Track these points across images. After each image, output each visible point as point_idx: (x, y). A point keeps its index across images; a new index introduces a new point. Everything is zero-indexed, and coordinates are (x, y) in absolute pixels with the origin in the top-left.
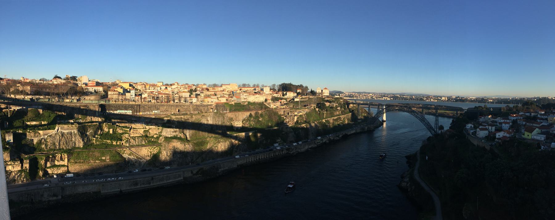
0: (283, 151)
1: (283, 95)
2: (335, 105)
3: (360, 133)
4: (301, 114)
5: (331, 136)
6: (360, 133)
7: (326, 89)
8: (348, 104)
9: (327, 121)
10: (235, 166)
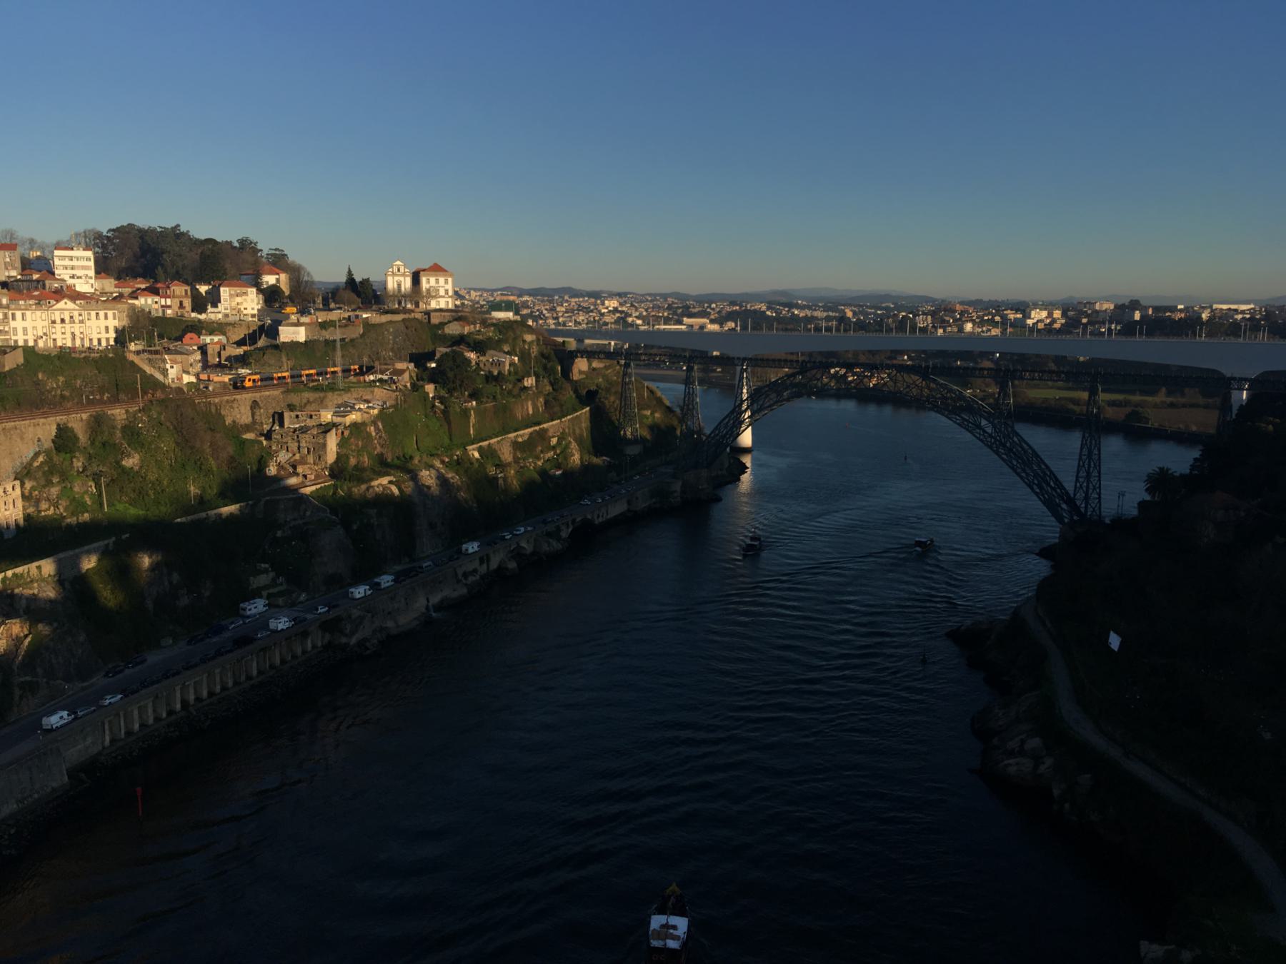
0: (305, 634)
1: (199, 305)
2: (508, 361)
4: (353, 417)
5: (524, 536)
7: (437, 269)
8: (566, 358)
9: (488, 454)
10: (59, 780)
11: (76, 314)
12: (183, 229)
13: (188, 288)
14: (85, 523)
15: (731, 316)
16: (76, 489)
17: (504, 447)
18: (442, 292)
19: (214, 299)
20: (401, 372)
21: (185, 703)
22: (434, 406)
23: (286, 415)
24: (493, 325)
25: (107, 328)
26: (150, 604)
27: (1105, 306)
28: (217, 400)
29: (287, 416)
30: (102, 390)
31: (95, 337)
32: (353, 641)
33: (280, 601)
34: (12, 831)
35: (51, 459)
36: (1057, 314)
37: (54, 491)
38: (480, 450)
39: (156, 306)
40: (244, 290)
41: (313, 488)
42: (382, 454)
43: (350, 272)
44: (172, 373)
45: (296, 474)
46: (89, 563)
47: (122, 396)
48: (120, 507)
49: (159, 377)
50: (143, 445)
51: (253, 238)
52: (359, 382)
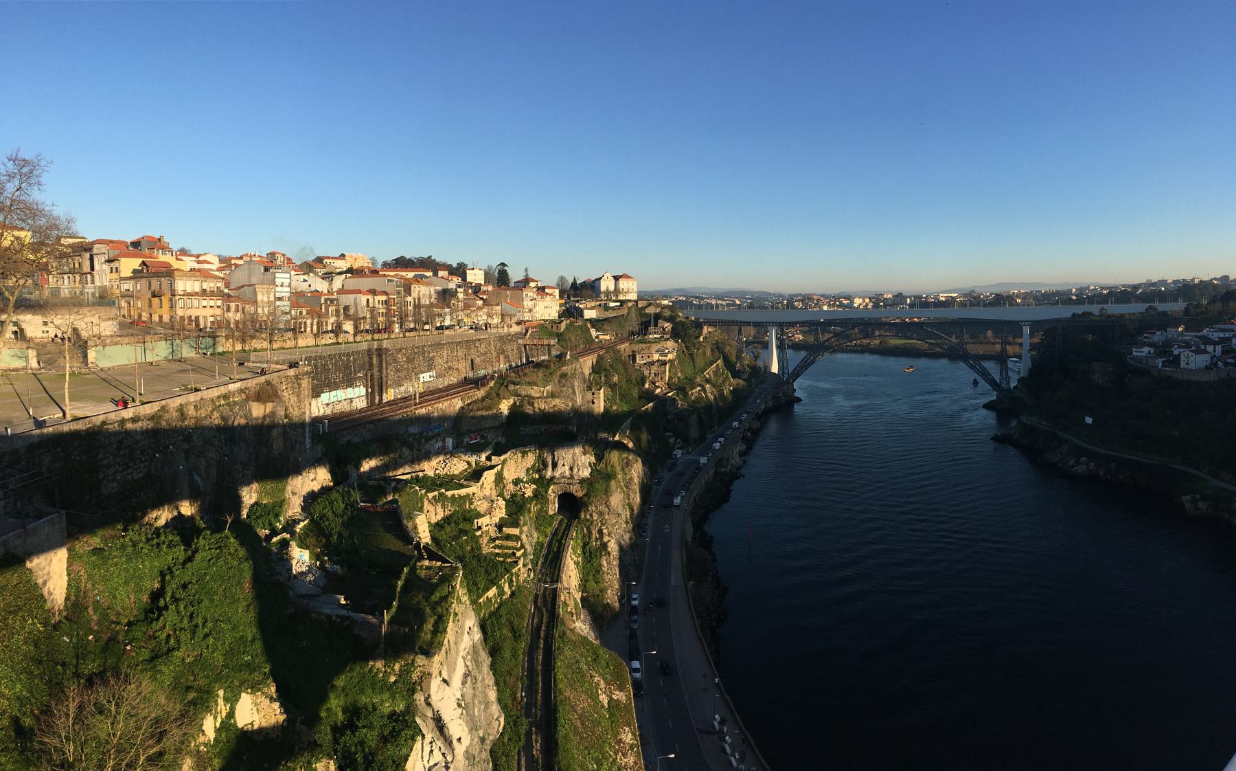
4: (670, 356)
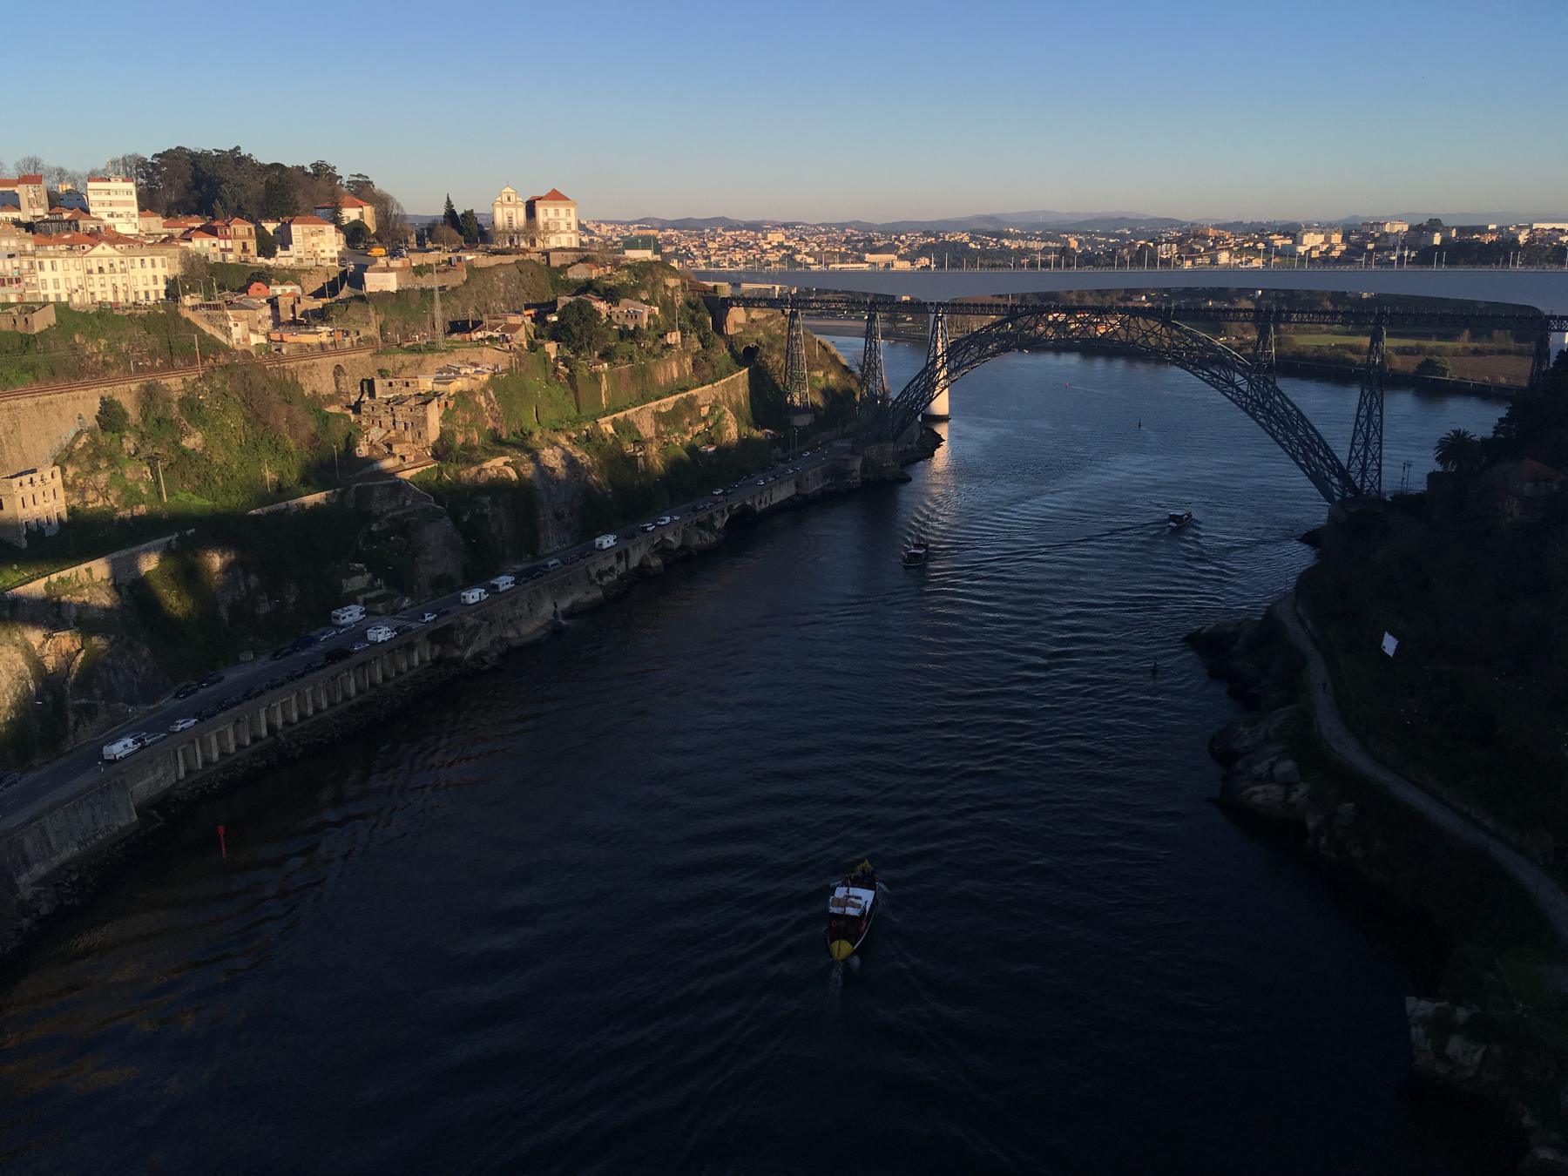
0: (410, 647)
1: (266, 248)
2: (645, 313)
3: (826, 499)
4: (459, 384)
5: (669, 527)
6: (826, 499)
7: (555, 196)
10: (127, 818)
11: (116, 261)
12: (244, 152)
13: (252, 226)
14: (141, 516)
15: (924, 251)
16: (128, 475)
17: (644, 420)
18: (563, 227)
19: (286, 242)
20: (515, 328)
21: (271, 728)
22: (556, 370)
23: (377, 382)
24: (628, 267)
25: (155, 278)
26: (224, 613)
27: (1397, 228)
28: (292, 365)
29: (379, 384)
30: (153, 354)
31: (141, 289)
32: (468, 654)
33: (380, 607)
34: (75, 878)
35: (96, 440)
36: (1336, 238)
37: (102, 478)
38: (614, 422)
39: (215, 250)
40: (320, 227)
41: (414, 472)
42: (495, 430)
43: (449, 201)
44: (237, 332)
45: (391, 455)
46: (149, 563)
47: (178, 362)
48: (182, 497)
49: (222, 338)
50: (205, 422)
51: (330, 162)
52: (464, 341)
